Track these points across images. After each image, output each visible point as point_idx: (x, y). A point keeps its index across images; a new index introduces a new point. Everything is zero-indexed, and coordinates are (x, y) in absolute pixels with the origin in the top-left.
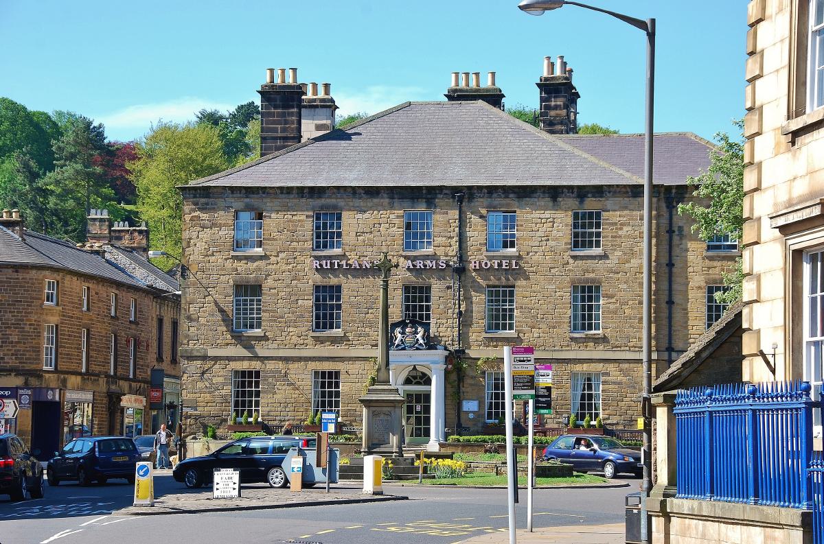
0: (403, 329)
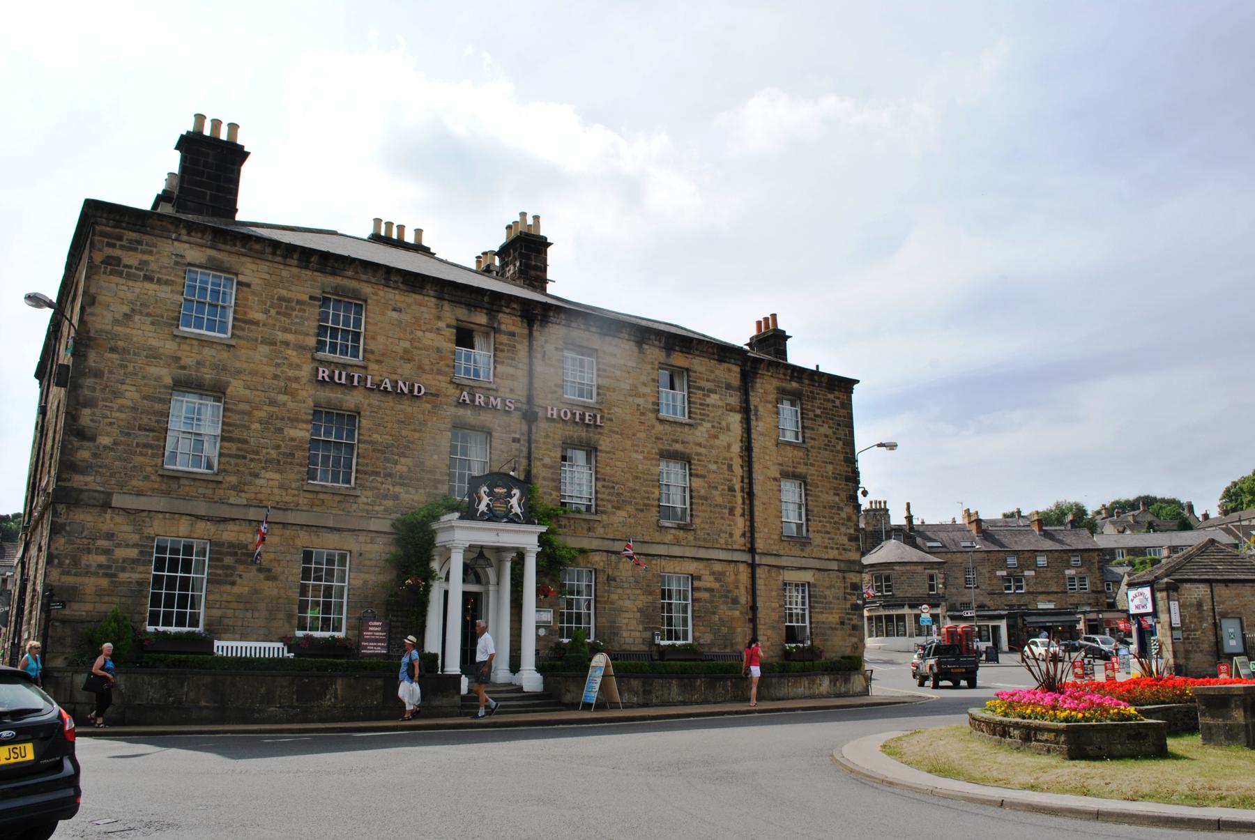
0: (491, 487)
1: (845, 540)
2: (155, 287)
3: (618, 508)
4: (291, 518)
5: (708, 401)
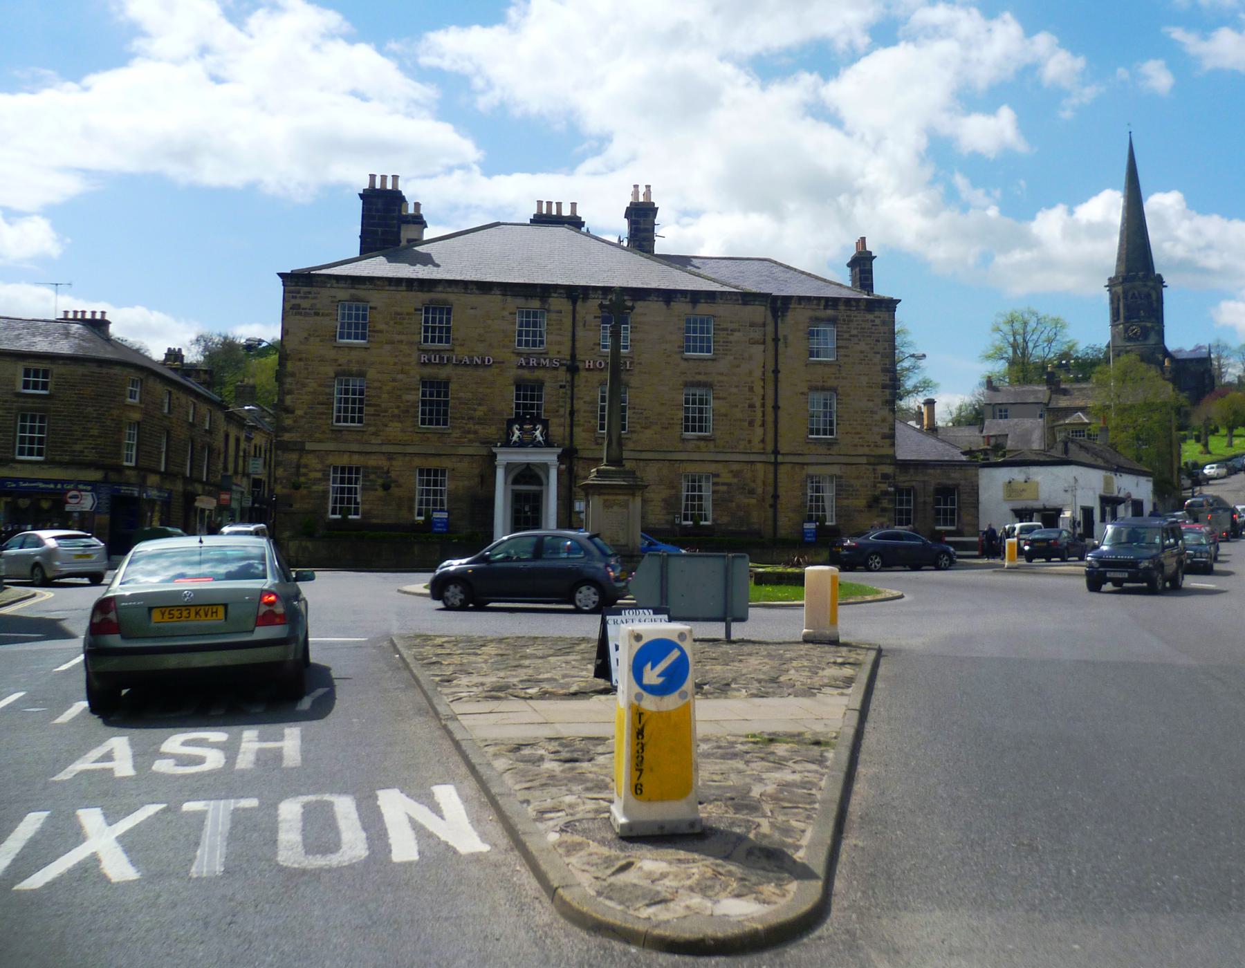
1: (878, 439)
2: (322, 318)
3: (646, 428)
4: (410, 450)
5: (731, 338)
